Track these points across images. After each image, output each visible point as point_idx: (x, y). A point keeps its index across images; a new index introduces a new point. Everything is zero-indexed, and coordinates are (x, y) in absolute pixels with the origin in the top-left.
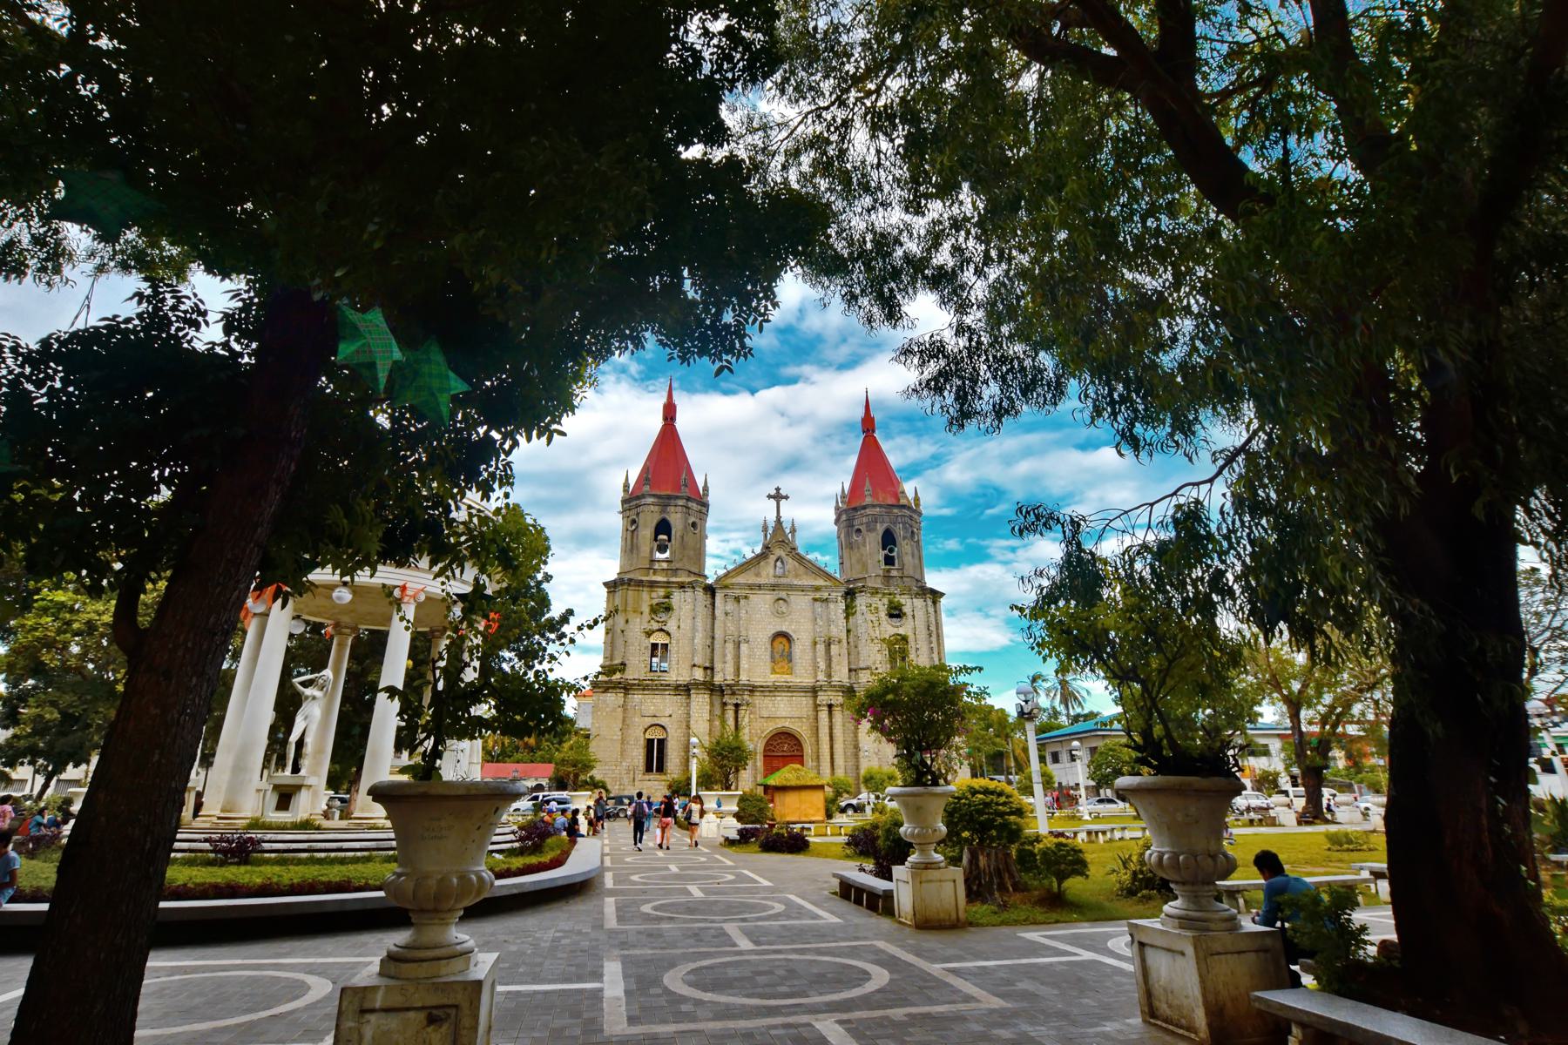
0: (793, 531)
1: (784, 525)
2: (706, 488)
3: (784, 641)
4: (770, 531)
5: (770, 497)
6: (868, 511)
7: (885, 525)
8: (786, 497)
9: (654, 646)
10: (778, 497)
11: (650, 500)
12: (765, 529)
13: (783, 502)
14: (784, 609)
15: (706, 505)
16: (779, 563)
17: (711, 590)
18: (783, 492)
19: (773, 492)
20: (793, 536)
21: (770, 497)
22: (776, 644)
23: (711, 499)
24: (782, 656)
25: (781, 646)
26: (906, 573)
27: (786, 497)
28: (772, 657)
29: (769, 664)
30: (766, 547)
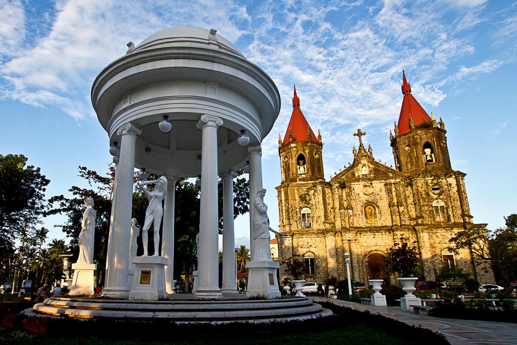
3: (371, 207)
8: (364, 134)
9: (304, 215)
10: (360, 134)
11: (293, 145)
13: (363, 137)
15: (321, 145)
17: (329, 185)
20: (371, 153)
21: (355, 135)
22: (367, 209)
23: (323, 141)
24: (371, 215)
25: (370, 211)
28: (366, 216)
29: (365, 220)
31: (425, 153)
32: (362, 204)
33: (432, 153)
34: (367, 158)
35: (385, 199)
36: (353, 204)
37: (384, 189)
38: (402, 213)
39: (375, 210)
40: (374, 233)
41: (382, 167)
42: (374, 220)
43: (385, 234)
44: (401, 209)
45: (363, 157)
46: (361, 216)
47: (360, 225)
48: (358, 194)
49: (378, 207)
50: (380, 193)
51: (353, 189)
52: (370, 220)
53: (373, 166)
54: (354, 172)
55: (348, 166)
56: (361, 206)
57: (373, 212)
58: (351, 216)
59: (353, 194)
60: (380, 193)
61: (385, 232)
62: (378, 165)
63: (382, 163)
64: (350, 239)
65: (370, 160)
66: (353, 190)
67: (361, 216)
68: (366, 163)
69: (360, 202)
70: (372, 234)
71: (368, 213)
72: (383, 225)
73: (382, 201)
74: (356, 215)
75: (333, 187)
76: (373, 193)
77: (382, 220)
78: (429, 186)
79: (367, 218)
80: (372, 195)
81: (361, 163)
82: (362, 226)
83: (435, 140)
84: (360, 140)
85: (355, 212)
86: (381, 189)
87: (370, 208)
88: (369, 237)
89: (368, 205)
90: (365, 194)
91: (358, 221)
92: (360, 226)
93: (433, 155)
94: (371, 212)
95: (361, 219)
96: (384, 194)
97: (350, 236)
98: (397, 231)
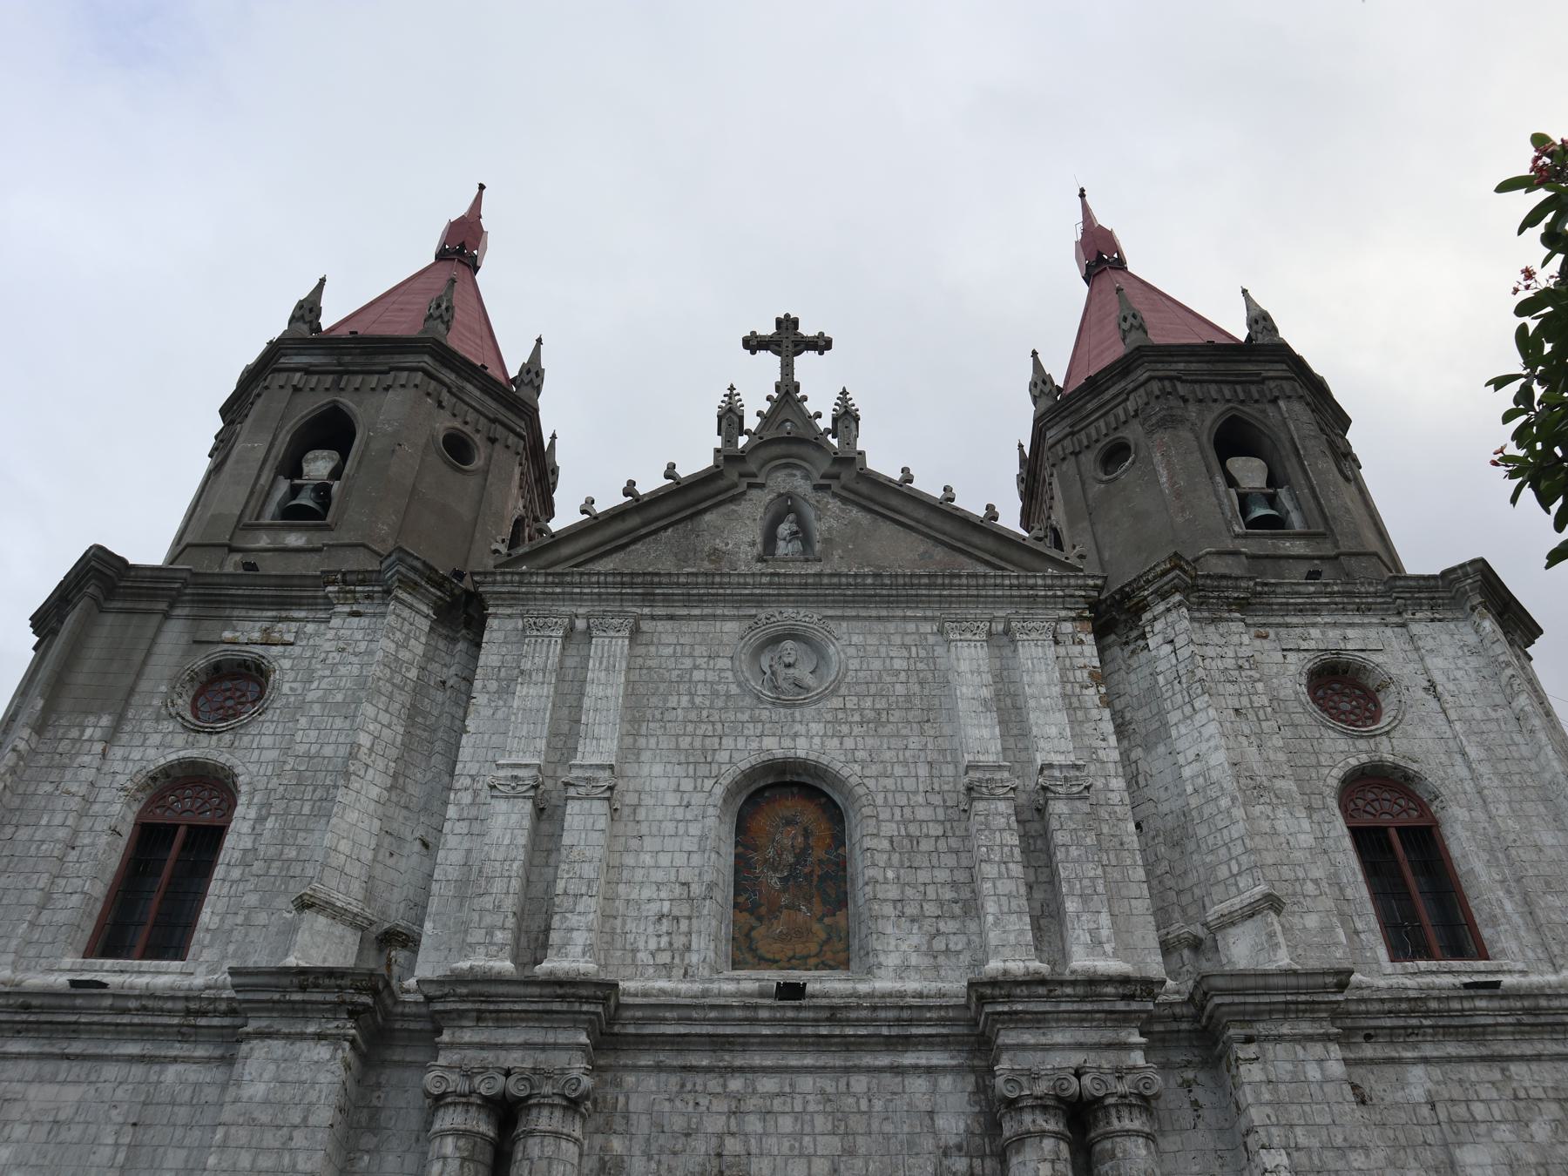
0: (846, 417)
1: (810, 407)
3: (809, 814)
4: (751, 423)
5: (754, 344)
6: (1141, 374)
7: (1219, 408)
8: (821, 344)
12: (730, 418)
14: (803, 672)
16: (784, 529)
18: (807, 329)
19: (768, 329)
21: (754, 344)
25: (789, 838)
26: (1346, 545)
27: (821, 344)
30: (727, 457)
31: (1231, 482)
33: (1272, 481)
42: (816, 927)
52: (779, 928)
55: (651, 482)
57: (819, 853)
63: (928, 484)
64: (516, 1088)
79: (753, 910)
84: (787, 369)
87: (789, 822)
88: (736, 1084)
93: (1283, 493)
97: (512, 1059)
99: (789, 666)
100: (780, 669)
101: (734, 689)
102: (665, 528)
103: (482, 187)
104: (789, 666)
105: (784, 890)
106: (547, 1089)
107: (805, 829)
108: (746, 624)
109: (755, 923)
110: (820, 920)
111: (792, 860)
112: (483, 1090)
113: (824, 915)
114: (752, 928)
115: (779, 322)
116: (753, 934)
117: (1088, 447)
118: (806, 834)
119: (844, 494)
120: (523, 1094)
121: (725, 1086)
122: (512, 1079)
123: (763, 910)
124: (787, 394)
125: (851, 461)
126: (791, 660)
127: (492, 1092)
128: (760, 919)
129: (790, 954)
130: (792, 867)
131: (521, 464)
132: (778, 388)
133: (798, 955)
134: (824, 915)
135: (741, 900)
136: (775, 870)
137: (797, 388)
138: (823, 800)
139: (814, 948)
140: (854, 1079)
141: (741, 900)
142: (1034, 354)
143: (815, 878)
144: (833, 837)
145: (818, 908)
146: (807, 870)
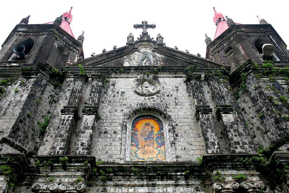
2: (82, 38)
5: (137, 27)
21: (137, 27)
32: (126, 111)
34: (152, 44)
35: (187, 104)
36: (105, 110)
37: (183, 87)
38: (231, 127)
39: (161, 128)
40: (150, 178)
41: (180, 56)
42: (155, 150)
43: (188, 185)
44: (228, 118)
45: (144, 43)
46: (119, 136)
47: (111, 156)
48: (123, 93)
49: (167, 118)
50: (175, 94)
51: (113, 85)
53: (163, 56)
54: (123, 61)
55: (109, 49)
56: (125, 115)
58: (87, 128)
59: (110, 93)
60: (175, 94)
61: (187, 178)
62: (173, 53)
65: (157, 47)
66: (112, 87)
67: (119, 136)
68: (149, 51)
69: (124, 108)
70: (145, 182)
71: (142, 135)
72: (180, 160)
73: (179, 107)
74: (106, 132)
75: (68, 79)
76: (158, 92)
77: (179, 148)
78: (283, 88)
80: (155, 96)
81: (139, 51)
82: (117, 161)
83: (271, 37)
85: (106, 126)
86: (176, 87)
87: (147, 125)
89: (143, 117)
90: (138, 94)
91: (107, 148)
92: (111, 160)
94: (152, 131)
95: (118, 143)
96: (183, 94)
98: (223, 168)
99: (146, 87)
100: (144, 89)
101: (131, 93)
102: (113, 59)
103: (72, 8)
104: (146, 87)
105: (146, 141)
106: (71, 188)
107: (152, 126)
108: (135, 79)
109: (137, 149)
110: (157, 148)
111: (148, 134)
112: (51, 189)
113: (157, 147)
114: (137, 151)
115: (142, 22)
116: (137, 152)
117: (221, 50)
118: (152, 127)
119: (160, 52)
120: (65, 189)
121: (128, 190)
122: (61, 185)
123: (140, 146)
124: (145, 34)
125: (162, 45)
126: (147, 86)
127: (53, 189)
128: (139, 148)
129: (148, 157)
130: (148, 136)
131: (77, 57)
132: (142, 33)
133: (150, 158)
134: (157, 147)
135: (133, 143)
136: (143, 136)
137: (147, 33)
138: (156, 119)
139: (155, 156)
140: (168, 188)
141: (133, 143)
142: (206, 35)
143: (155, 138)
144: (160, 128)
145: (156, 145)
146: (152, 136)
